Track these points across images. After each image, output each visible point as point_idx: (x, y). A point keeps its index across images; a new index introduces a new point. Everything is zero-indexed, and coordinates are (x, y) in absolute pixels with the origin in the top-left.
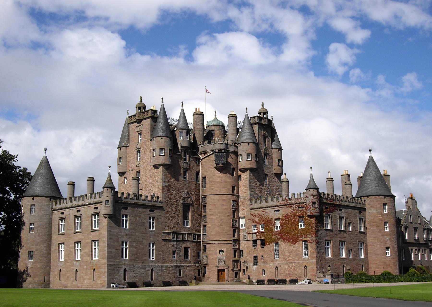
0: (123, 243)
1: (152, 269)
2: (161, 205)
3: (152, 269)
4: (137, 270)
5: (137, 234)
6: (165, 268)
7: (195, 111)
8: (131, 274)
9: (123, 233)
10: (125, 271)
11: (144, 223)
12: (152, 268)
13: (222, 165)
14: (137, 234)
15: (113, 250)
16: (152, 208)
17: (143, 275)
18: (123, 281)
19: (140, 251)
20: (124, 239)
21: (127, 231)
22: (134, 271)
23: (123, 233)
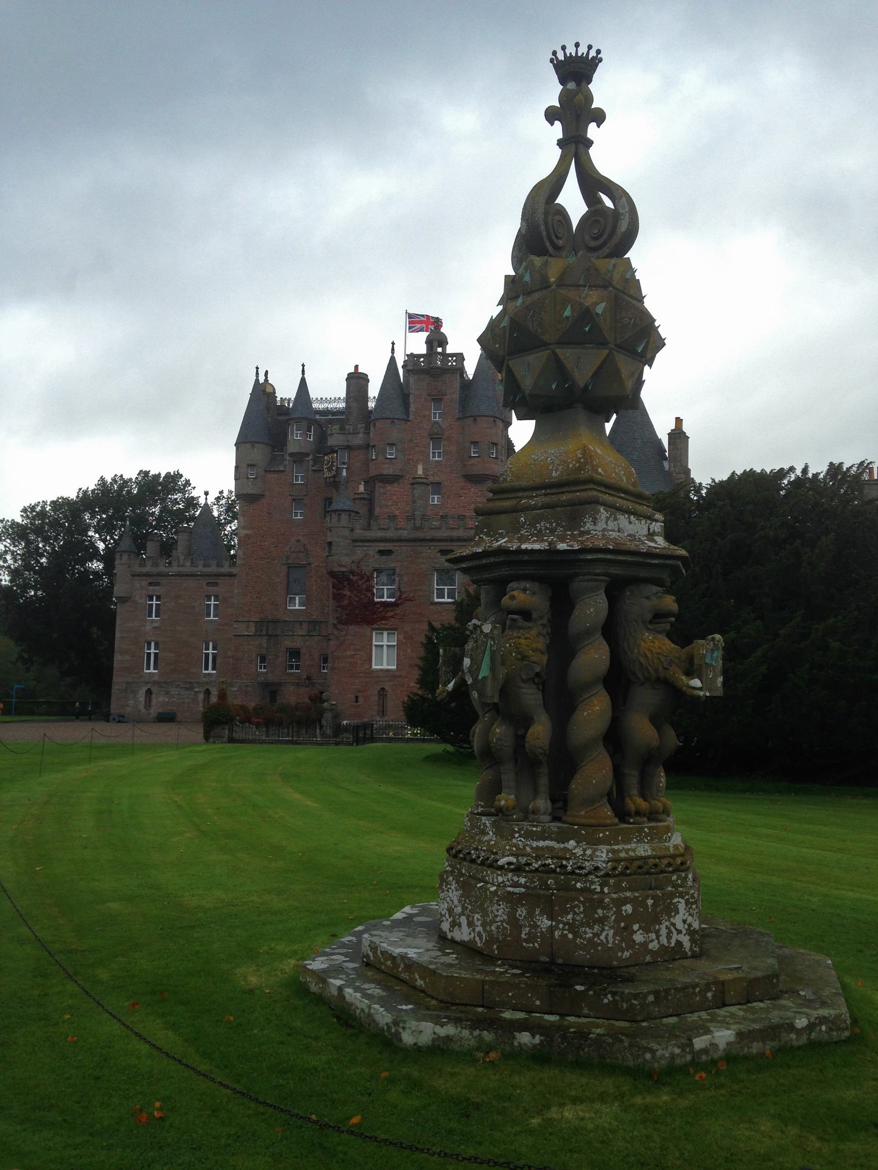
0: (149, 644)
1: (207, 690)
2: (234, 571)
3: (207, 690)
4: (174, 691)
5: (179, 628)
6: (236, 689)
7: (353, 371)
8: (161, 699)
9: (148, 627)
10: (149, 692)
11: (194, 607)
12: (206, 687)
13: (332, 480)
14: (179, 628)
15: (127, 657)
16: (213, 579)
17: (187, 700)
18: (143, 710)
19: (183, 658)
20: (149, 639)
21: (156, 625)
22: (167, 693)
23: (148, 627)
